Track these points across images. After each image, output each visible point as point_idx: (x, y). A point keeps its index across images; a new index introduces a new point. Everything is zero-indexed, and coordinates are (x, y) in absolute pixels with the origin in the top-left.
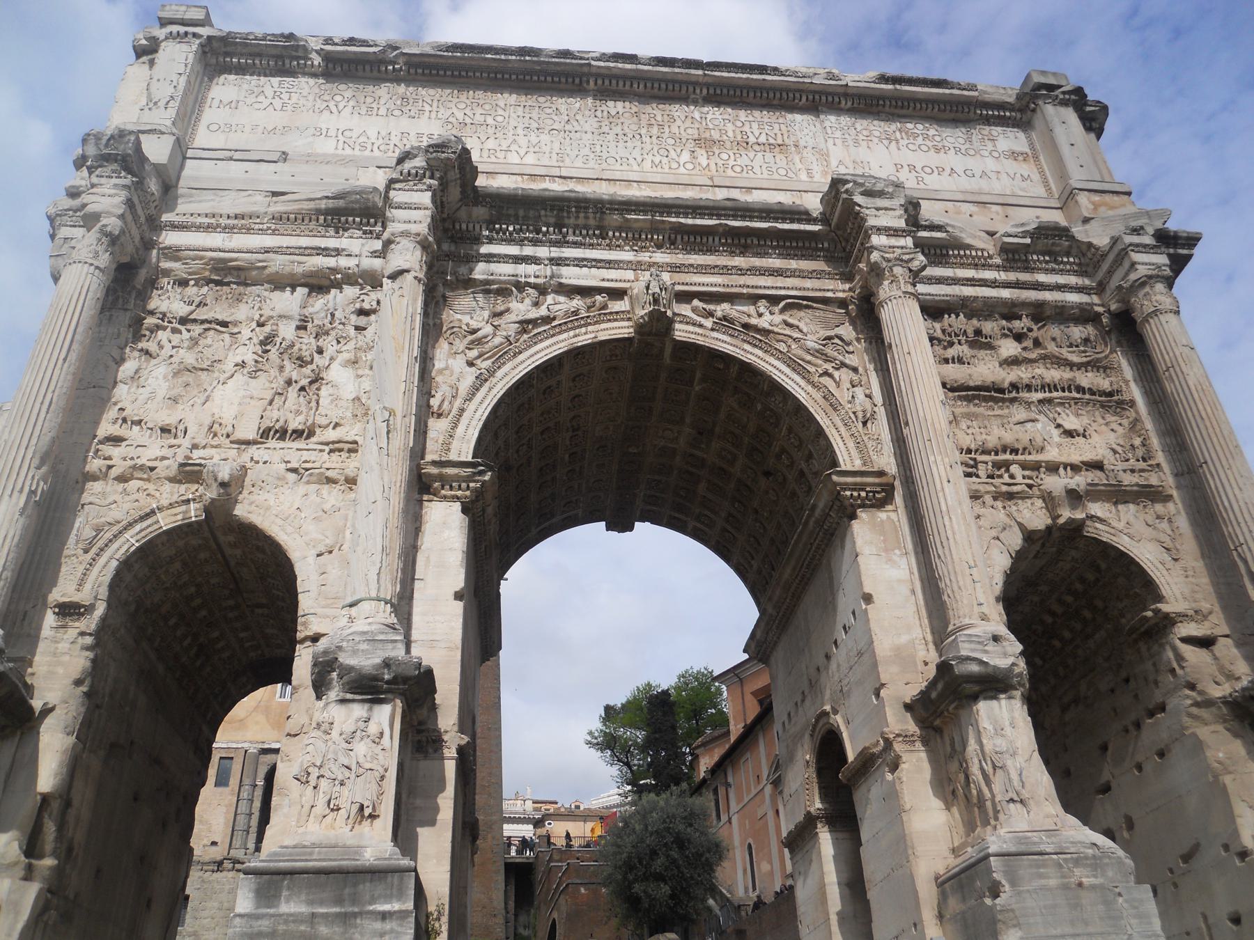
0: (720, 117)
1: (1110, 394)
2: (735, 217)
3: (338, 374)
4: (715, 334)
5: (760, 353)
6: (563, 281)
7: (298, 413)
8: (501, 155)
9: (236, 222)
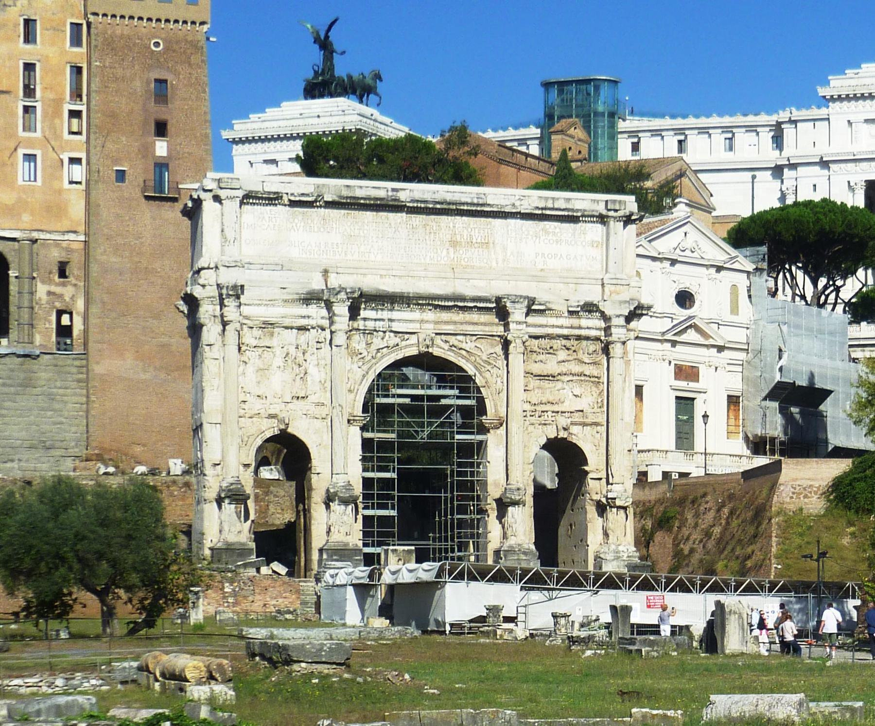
0: (461, 226)
1: (597, 377)
2: (461, 302)
3: (312, 370)
4: (449, 353)
5: (464, 361)
6: (393, 329)
7: (302, 389)
8: (367, 255)
9: (269, 302)
